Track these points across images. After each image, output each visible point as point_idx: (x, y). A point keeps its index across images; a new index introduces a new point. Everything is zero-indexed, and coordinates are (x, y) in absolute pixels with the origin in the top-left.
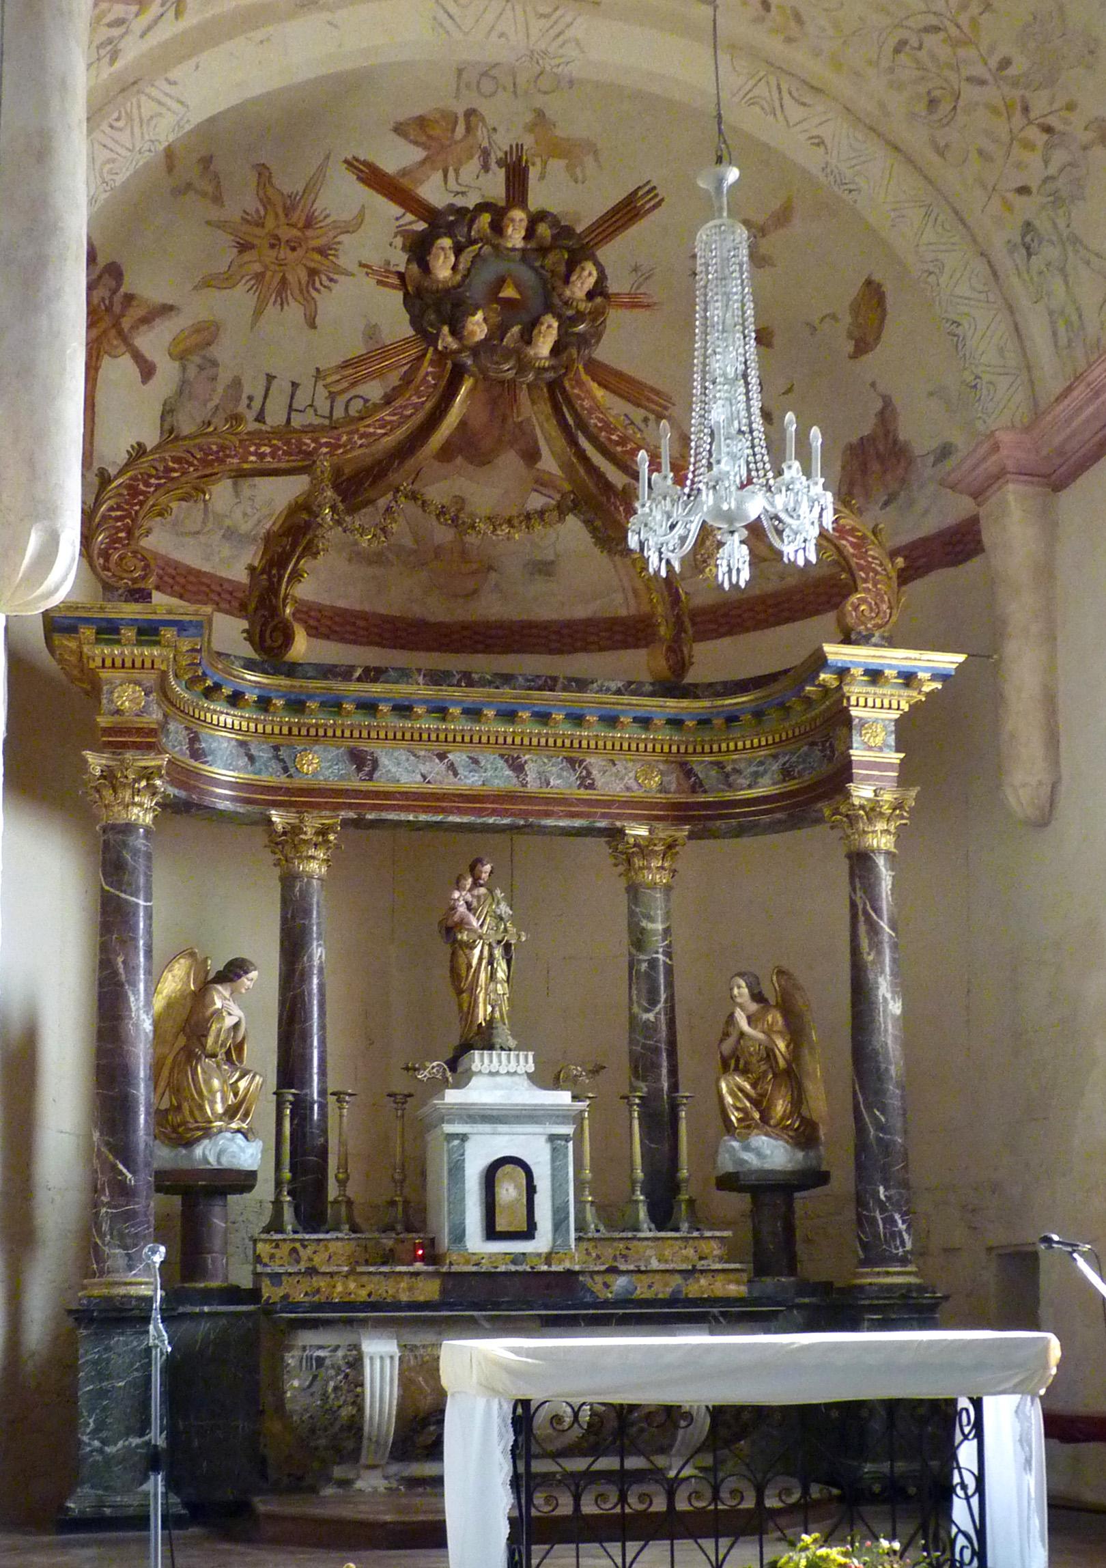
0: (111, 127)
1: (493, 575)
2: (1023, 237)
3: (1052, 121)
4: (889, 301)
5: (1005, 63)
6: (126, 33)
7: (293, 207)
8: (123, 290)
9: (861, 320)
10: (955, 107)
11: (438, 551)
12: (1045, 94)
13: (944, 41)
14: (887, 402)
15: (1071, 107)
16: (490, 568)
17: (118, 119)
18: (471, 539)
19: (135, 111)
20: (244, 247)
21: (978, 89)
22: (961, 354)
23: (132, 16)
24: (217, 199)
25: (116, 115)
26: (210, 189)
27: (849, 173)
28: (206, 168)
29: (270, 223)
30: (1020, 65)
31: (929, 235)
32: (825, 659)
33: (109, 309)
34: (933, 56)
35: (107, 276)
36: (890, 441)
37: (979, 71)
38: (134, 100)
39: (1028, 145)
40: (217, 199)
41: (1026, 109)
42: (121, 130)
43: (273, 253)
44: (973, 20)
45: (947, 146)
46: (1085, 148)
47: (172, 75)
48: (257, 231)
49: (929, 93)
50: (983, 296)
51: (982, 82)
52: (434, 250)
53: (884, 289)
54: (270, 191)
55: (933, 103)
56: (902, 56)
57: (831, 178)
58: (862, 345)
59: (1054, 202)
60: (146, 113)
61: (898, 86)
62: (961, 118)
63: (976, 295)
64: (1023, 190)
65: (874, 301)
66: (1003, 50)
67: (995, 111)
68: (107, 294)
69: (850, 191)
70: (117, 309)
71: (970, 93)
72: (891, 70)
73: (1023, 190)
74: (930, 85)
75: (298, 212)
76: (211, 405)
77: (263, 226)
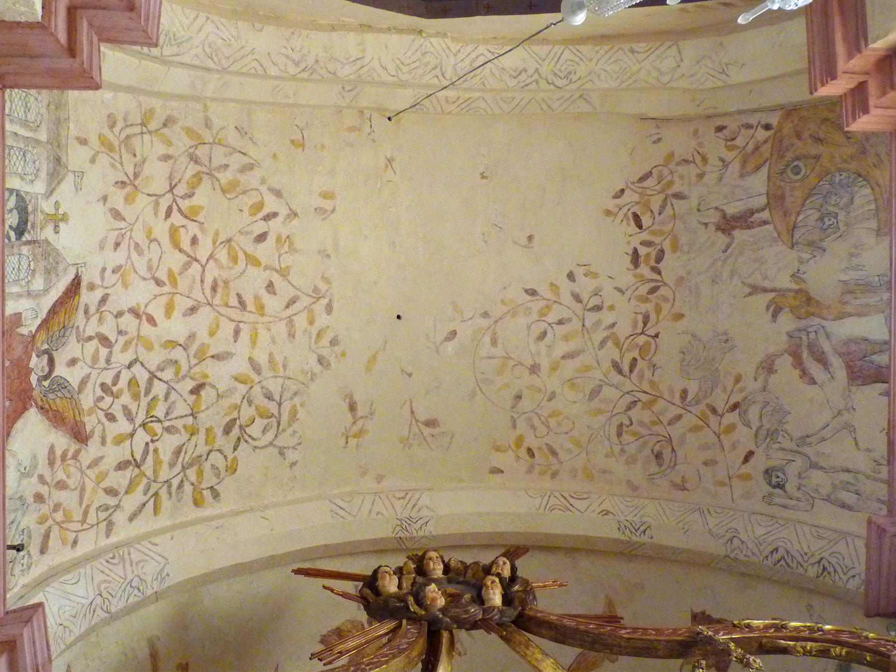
0: (107, 562)
2: (770, 484)
10: (673, 450)
12: (718, 391)
13: (642, 408)
15: (738, 379)
17: (113, 558)
19: (126, 556)
21: (679, 425)
22: (794, 565)
25: (111, 555)
30: (693, 388)
34: (641, 424)
38: (126, 550)
39: (731, 428)
41: (714, 411)
42: (115, 564)
44: (652, 383)
46: (764, 389)
49: (652, 451)
51: (679, 417)
52: (380, 575)
53: (707, 613)
55: (658, 456)
56: (625, 436)
57: (627, 532)
59: (772, 439)
60: (135, 560)
67: (696, 429)
69: (644, 532)
71: (676, 431)
72: (623, 450)
74: (651, 445)
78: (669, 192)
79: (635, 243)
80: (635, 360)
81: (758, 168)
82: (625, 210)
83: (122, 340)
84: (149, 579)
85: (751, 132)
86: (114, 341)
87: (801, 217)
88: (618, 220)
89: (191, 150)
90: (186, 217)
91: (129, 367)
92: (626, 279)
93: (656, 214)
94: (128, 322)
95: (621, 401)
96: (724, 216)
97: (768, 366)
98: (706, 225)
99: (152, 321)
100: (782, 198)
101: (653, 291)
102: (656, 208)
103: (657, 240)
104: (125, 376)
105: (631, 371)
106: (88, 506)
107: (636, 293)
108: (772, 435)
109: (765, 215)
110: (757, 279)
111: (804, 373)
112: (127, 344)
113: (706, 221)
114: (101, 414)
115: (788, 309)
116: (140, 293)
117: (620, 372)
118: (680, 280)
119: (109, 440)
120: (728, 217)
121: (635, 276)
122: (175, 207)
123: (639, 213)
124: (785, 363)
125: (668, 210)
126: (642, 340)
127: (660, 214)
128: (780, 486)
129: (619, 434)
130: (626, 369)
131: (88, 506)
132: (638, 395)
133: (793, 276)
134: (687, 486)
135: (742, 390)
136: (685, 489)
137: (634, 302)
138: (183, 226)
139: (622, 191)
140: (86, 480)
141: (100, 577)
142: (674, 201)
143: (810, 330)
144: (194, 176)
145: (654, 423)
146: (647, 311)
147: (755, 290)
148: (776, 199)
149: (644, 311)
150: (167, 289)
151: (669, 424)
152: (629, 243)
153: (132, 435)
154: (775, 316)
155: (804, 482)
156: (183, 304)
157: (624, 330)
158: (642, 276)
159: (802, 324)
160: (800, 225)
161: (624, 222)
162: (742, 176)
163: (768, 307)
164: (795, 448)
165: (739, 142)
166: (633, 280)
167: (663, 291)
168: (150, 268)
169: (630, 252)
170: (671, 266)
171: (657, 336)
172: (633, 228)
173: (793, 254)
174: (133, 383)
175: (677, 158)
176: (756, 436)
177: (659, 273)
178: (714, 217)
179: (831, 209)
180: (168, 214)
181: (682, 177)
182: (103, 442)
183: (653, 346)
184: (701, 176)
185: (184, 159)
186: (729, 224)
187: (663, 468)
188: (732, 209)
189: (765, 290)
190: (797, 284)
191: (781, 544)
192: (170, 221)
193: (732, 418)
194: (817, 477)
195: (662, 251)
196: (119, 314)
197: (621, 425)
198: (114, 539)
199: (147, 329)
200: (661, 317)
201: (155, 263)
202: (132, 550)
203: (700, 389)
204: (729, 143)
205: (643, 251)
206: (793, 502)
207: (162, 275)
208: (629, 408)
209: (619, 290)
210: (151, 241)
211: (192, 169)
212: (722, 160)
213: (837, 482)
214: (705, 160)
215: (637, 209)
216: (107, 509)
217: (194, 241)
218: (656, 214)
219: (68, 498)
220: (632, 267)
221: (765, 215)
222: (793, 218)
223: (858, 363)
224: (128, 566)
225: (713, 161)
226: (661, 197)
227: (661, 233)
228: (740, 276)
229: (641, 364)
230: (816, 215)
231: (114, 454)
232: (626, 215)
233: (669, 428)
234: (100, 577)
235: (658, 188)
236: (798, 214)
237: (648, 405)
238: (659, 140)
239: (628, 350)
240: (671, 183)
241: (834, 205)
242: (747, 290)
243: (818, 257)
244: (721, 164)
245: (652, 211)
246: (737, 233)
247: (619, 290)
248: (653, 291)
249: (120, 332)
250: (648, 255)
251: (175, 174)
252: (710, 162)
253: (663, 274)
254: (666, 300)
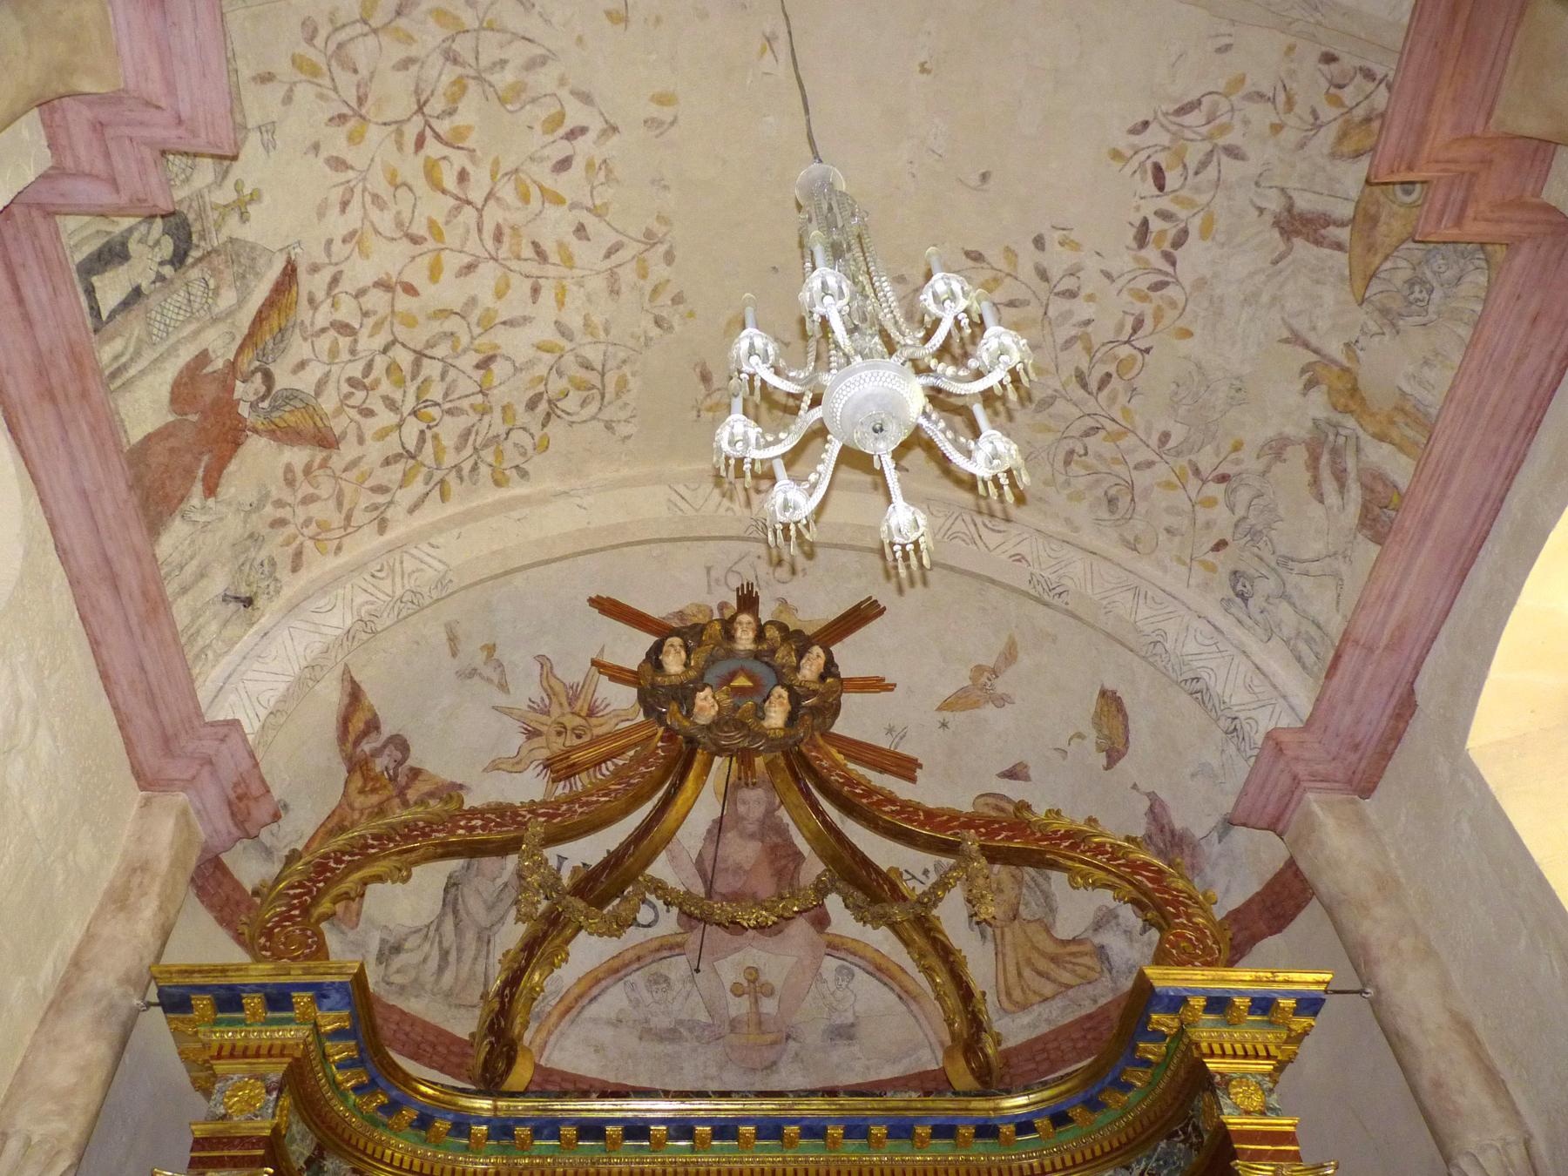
1: (792, 1044)
2: (1234, 588)
3: (1224, 469)
4: (1126, 701)
5: (1165, 437)
6: (391, 502)
7: (577, 697)
8: (410, 762)
9: (1106, 732)
11: (734, 1025)
12: (1208, 448)
13: (1105, 439)
14: (1153, 797)
15: (1237, 448)
16: (788, 1037)
18: (769, 1006)
19: (397, 565)
20: (532, 734)
23: (394, 487)
24: (503, 687)
26: (495, 677)
27: (1053, 577)
28: (490, 656)
29: (555, 711)
30: (1178, 434)
31: (1144, 612)
32: (1152, 987)
33: (393, 779)
34: (1099, 456)
35: (391, 747)
36: (1168, 834)
37: (1145, 455)
39: (1211, 502)
40: (503, 687)
41: (1197, 472)
43: (560, 740)
44: (1124, 410)
45: (1136, 539)
46: (1263, 474)
47: (433, 541)
48: (544, 718)
50: (1214, 648)
51: (1150, 464)
54: (553, 682)
55: (1112, 502)
58: (1113, 756)
61: (1076, 497)
62: (1142, 507)
63: (1206, 649)
64: (1220, 545)
65: (1113, 708)
66: (1159, 427)
67: (1169, 485)
68: (392, 766)
70: (402, 780)
71: (1142, 479)
72: (1068, 483)
73: (1220, 545)
74: (1105, 485)
75: (580, 703)
76: (500, 882)
77: (548, 713)
78: (1221, 141)
79: (1148, 210)
80: (1109, 375)
82: (1142, 156)
83: (370, 322)
84: (425, 590)
86: (357, 326)
87: (1388, 265)
88: (1128, 170)
89: (446, 45)
90: (447, 144)
91: (385, 351)
92: (1123, 262)
93: (1191, 172)
94: (377, 300)
95: (1077, 423)
96: (1290, 208)
97: (1277, 449)
98: (1261, 210)
99: (410, 290)
100: (1373, 220)
101: (1158, 286)
102: (1192, 160)
103: (1183, 214)
104: (380, 363)
105: (1100, 389)
106: (351, 510)
107: (1131, 285)
108: (1254, 534)
109: (1343, 234)
110: (1301, 325)
111: (1315, 482)
112: (378, 326)
113: (1264, 205)
114: (353, 413)
115: (1324, 388)
116: (388, 258)
117: (1084, 386)
118: (1201, 283)
119: (368, 436)
121: (1137, 259)
122: (428, 132)
123: (1164, 166)
124: (1297, 457)
125: (1211, 172)
126: (1124, 351)
127: (1196, 173)
128: (1243, 597)
129: (1067, 463)
130: (1093, 384)
131: (351, 510)
132: (1102, 420)
133: (1347, 345)
134: (1139, 547)
135: (1238, 462)
136: (1135, 550)
138: (444, 158)
139: (1146, 124)
140: (343, 484)
141: (361, 598)
142: (1225, 159)
143: (1342, 432)
144: (454, 83)
145: (1115, 461)
146: (1142, 314)
147: (1296, 339)
148: (1365, 219)
149: (1137, 312)
150: (430, 244)
151: (1136, 468)
152: (1138, 209)
153: (399, 426)
154: (1310, 385)
155: (1270, 608)
156: (452, 262)
157: (1102, 332)
158: (1147, 262)
159: (1337, 417)
160: (1382, 275)
161: (1138, 176)
163: (1303, 371)
164: (1273, 564)
166: (1133, 265)
167: (1171, 291)
168: (399, 224)
169: (1137, 223)
170: (1195, 258)
171: (1147, 351)
172: (1150, 187)
173: (1362, 315)
174: (392, 369)
175: (1248, 87)
176: (1236, 526)
177: (1174, 264)
178: (1274, 204)
179: (1429, 275)
180: (420, 143)
181: (1246, 122)
182: (361, 440)
183: (1139, 364)
185: (437, 60)
187: (1117, 516)
188: (1303, 203)
189: (1306, 345)
190: (1349, 359)
191: (1205, 676)
192: (422, 153)
193: (1215, 490)
194: (1284, 612)
195: (1185, 232)
196: (360, 293)
197: (1072, 452)
198: (390, 535)
199: (404, 302)
200: (1160, 327)
201: (406, 216)
202: (406, 557)
203: (1186, 440)
204: (1333, 90)
205: (1156, 225)
206: (1250, 622)
207: (419, 229)
208: (1087, 434)
209: (1108, 275)
210: (397, 187)
211: (450, 74)
212: (1314, 113)
213: (1303, 630)
214: (1290, 103)
215: (1162, 159)
216: (376, 508)
217: (463, 176)
218: (1191, 172)
219: (324, 511)
220: (1134, 245)
221: (1343, 234)
222: (1377, 260)
223: (1377, 510)
224: (398, 579)
225: (1301, 109)
226: (1207, 146)
227: (1189, 203)
228: (1283, 307)
229: (1115, 382)
230: (1406, 274)
231: (375, 451)
232: (1142, 164)
233: (1135, 474)
234: (361, 598)
235: (1205, 130)
236: (1386, 258)
237: (1114, 437)
238: (1228, 47)
239: (1102, 361)
240: (1224, 129)
241: (1434, 273)
242: (1286, 334)
243: (1387, 337)
244: (1311, 120)
245: (1185, 166)
246: (1298, 242)
247: (1108, 275)
248: (1158, 286)
249: (366, 314)
250: (1162, 233)
251: (422, 85)
252: (1297, 109)
253: (1178, 266)
254: (1173, 304)
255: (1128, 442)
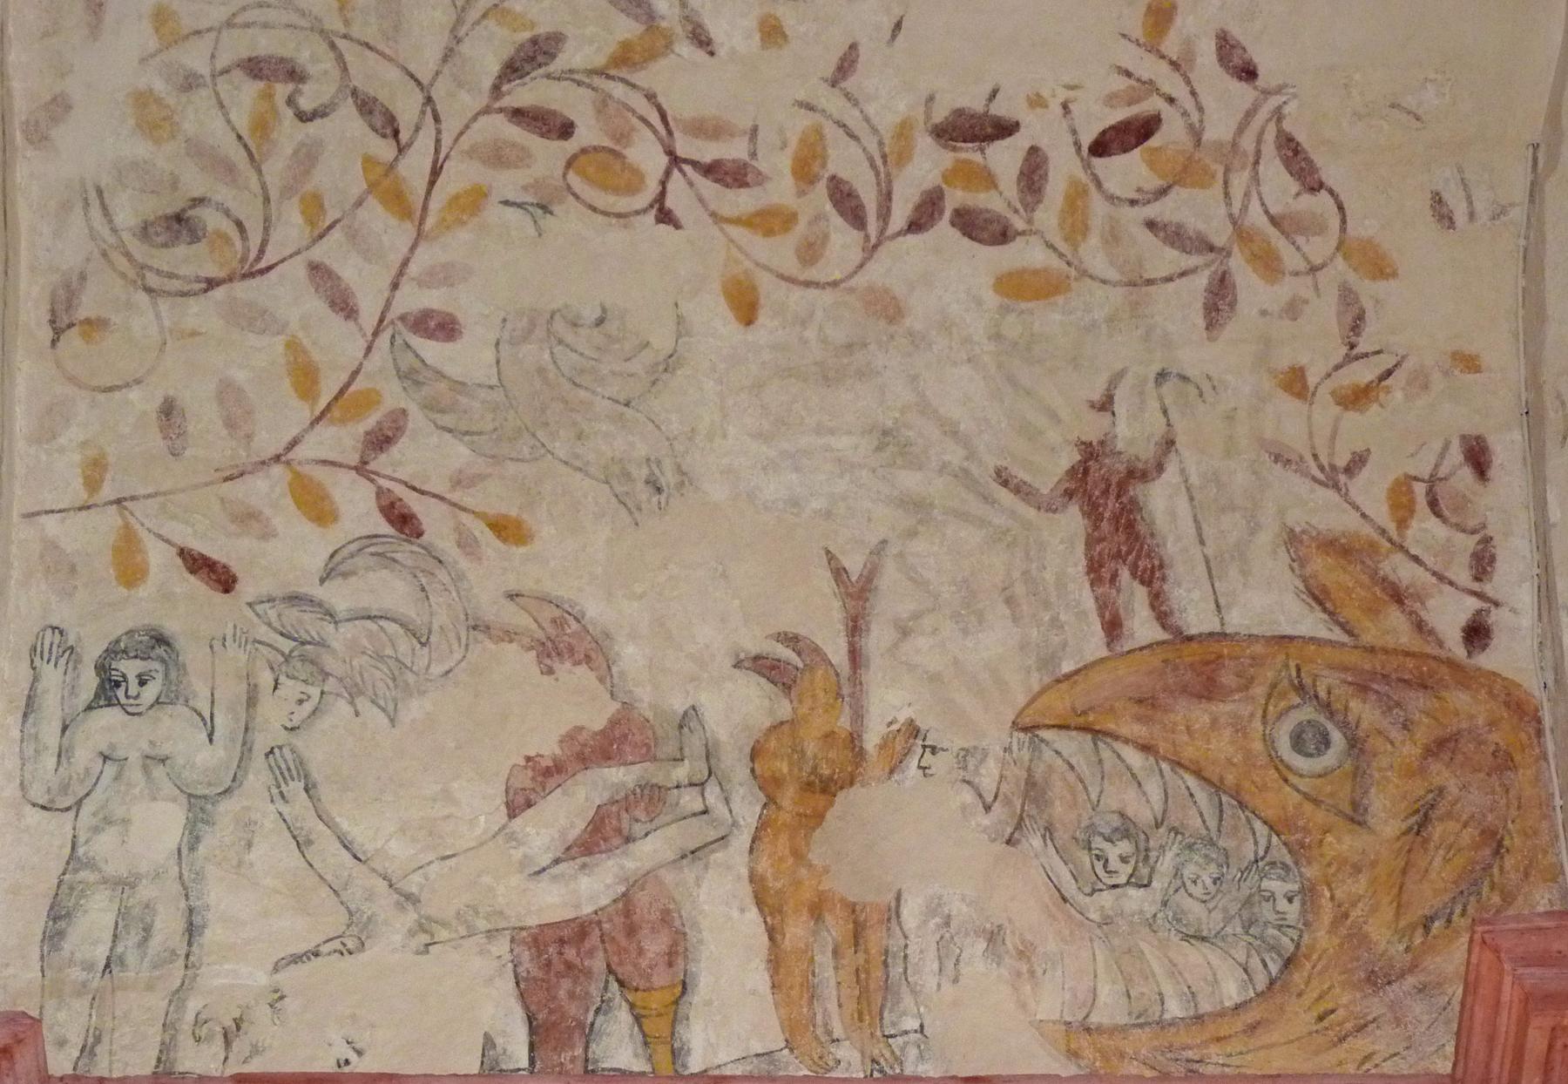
5: (445, 328)
13: (369, 162)
30: (463, 360)
34: (308, 157)
37: (367, 283)
44: (472, 202)
51: (344, 306)
55: (180, 224)
71: (287, 295)
72: (190, 83)
74: (223, 193)
78: (1238, 265)
79: (1037, 129)
80: (566, 130)
81: (1319, 597)
82: (1171, 83)
85: (1463, 576)
88: (1131, 57)
92: (889, 97)
93: (1151, 211)
95: (394, 74)
96: (1138, 474)
98: (1105, 405)
101: (845, 199)
102: (1177, 208)
103: (1048, 215)
105: (518, 115)
107: (830, 131)
113: (1120, 407)
117: (513, 70)
118: (888, 308)
120: (1137, 490)
121: (904, 130)
123: (1154, 142)
125: (1168, 259)
126: (647, 156)
127: (1151, 225)
129: (255, 67)
130: (524, 94)
137: (805, 120)
142: (1201, 281)
145: (313, 206)
146: (761, 179)
149: (762, 165)
151: (315, 268)
152: (1037, 102)
157: (682, 82)
158: (904, 157)
161: (1121, 83)
162: (1292, 539)
165: (1426, 530)
166: (887, 122)
167: (843, 241)
169: (1000, 109)
170: (947, 278)
171: (665, 216)
172: (1096, 119)
177: (915, 226)
178: (1132, 433)
183: (623, 204)
184: (1295, 383)
186: (1107, 494)
188: (1161, 502)
195: (1003, 236)
197: (295, 75)
200: (735, 232)
203: (459, 386)
204: (1420, 489)
205: (1004, 158)
208: (366, 106)
209: (846, 65)
212: (1358, 461)
215: (1172, 132)
218: (1151, 211)
220: (940, 114)
225: (1357, 428)
226: (1220, 234)
227: (1076, 228)
229: (548, 155)
232: (1150, 86)
237: (385, 186)
239: (603, 104)
244: (1342, 461)
245: (1163, 192)
247: (846, 65)
248: (845, 199)
250: (988, 180)
252: (1351, 418)
253: (912, 239)
254: (811, 252)
255: (392, 234)
